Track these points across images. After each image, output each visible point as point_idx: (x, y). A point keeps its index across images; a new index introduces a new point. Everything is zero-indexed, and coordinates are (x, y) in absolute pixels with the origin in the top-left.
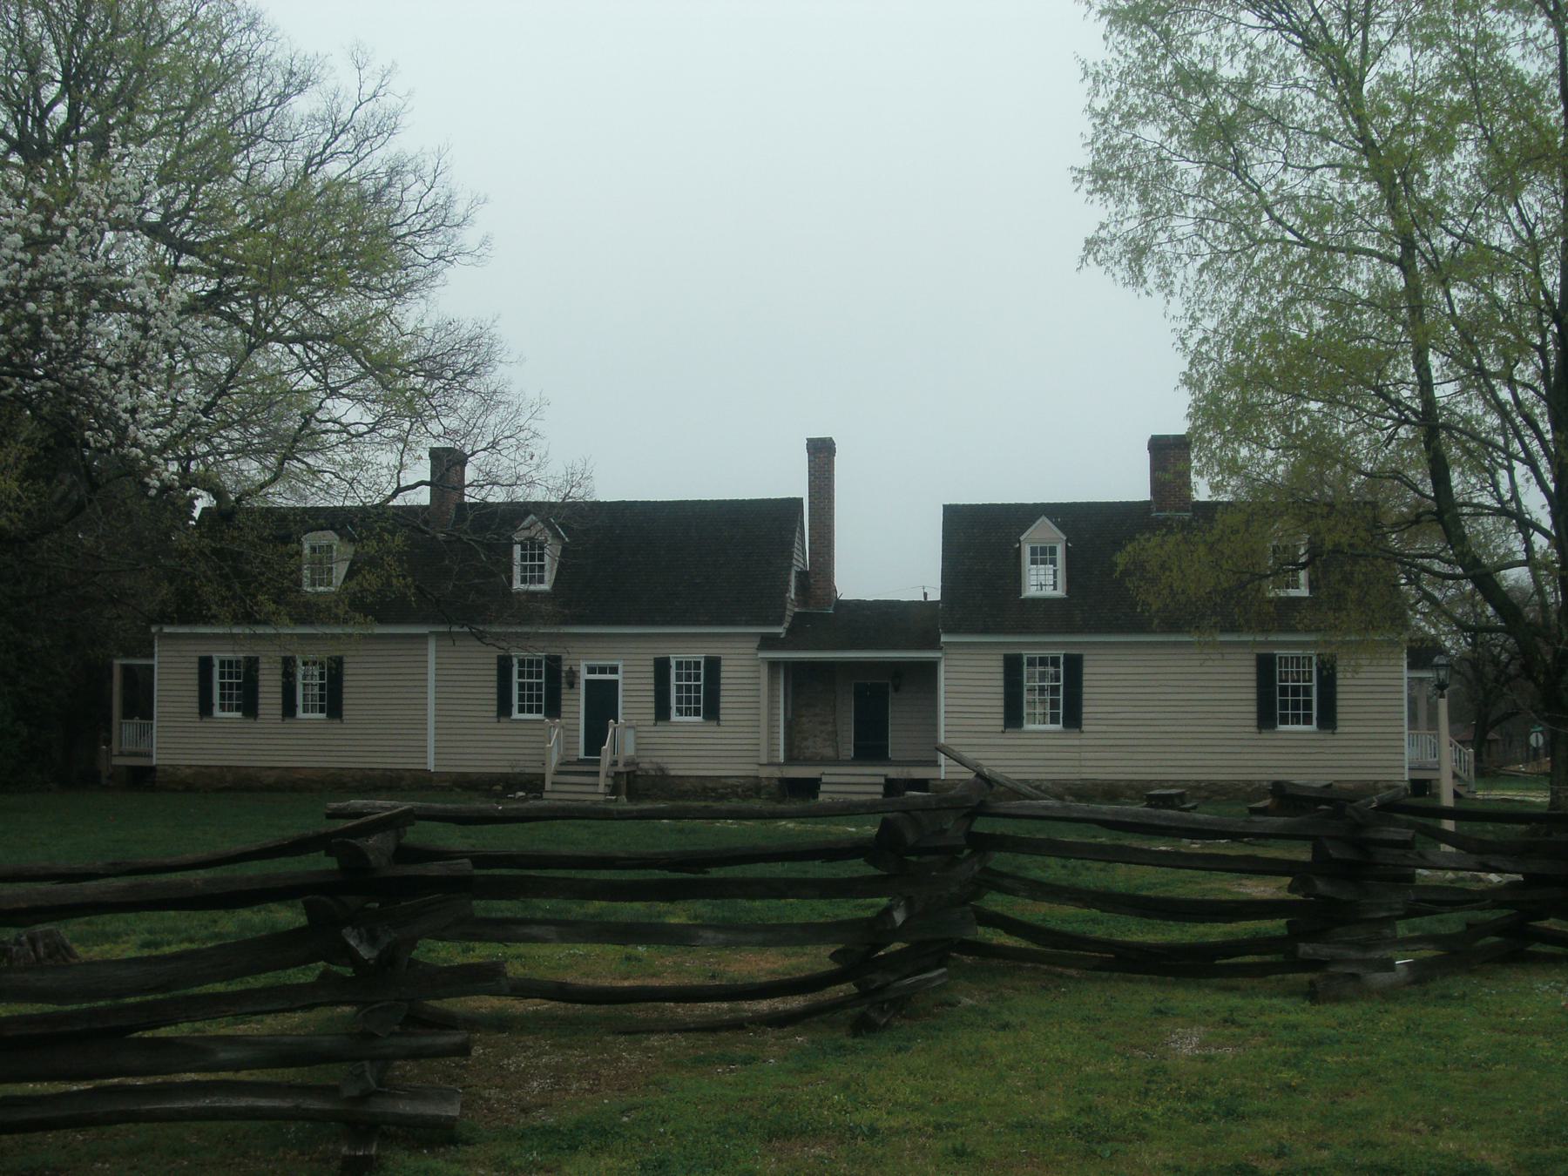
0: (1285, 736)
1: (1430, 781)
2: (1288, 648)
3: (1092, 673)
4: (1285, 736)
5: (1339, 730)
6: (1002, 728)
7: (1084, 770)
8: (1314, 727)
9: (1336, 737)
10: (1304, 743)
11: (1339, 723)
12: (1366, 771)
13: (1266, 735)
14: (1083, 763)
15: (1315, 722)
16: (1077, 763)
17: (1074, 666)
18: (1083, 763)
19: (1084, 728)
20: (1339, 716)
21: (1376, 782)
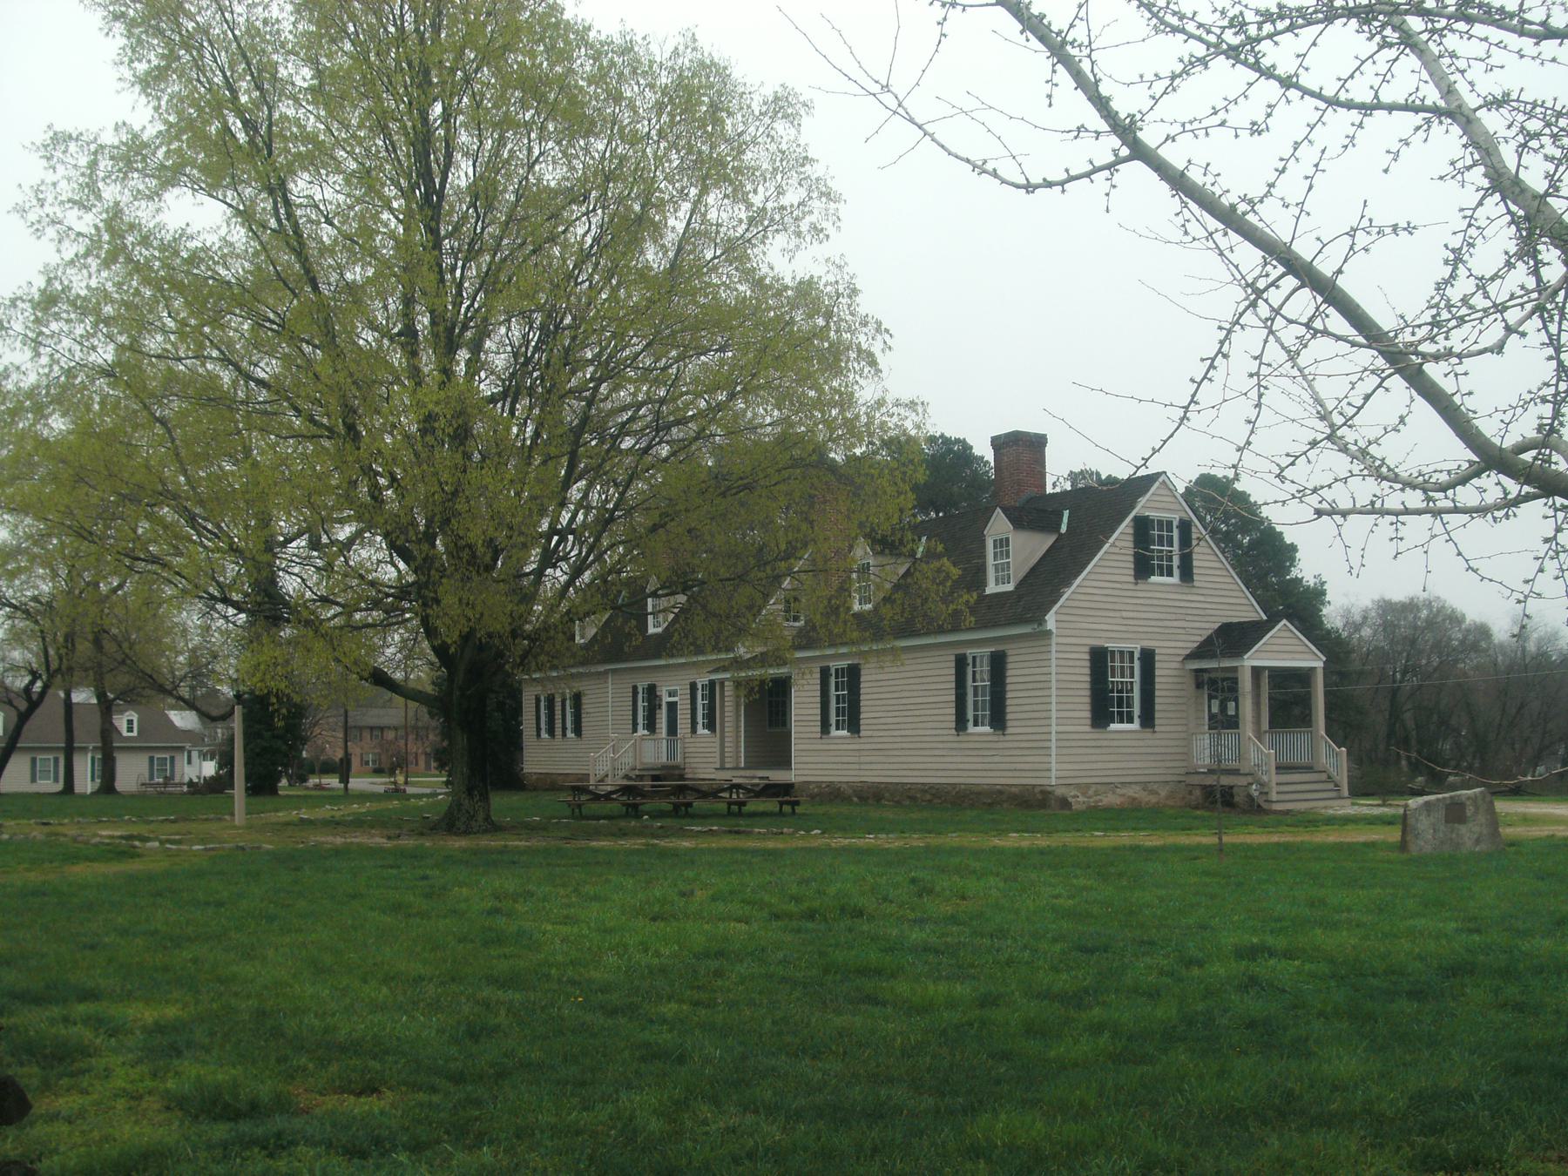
0: (977, 738)
1: (1231, 787)
2: (979, 647)
3: (868, 679)
4: (977, 738)
5: (1009, 731)
6: (819, 735)
7: (862, 773)
8: (1135, 726)
9: (1007, 738)
10: (984, 745)
11: (1009, 724)
12: (998, 774)
13: (1098, 734)
14: (863, 767)
15: (1137, 720)
16: (857, 766)
17: (853, 674)
18: (863, 767)
19: (1157, 729)
20: (1009, 717)
21: (1034, 786)
